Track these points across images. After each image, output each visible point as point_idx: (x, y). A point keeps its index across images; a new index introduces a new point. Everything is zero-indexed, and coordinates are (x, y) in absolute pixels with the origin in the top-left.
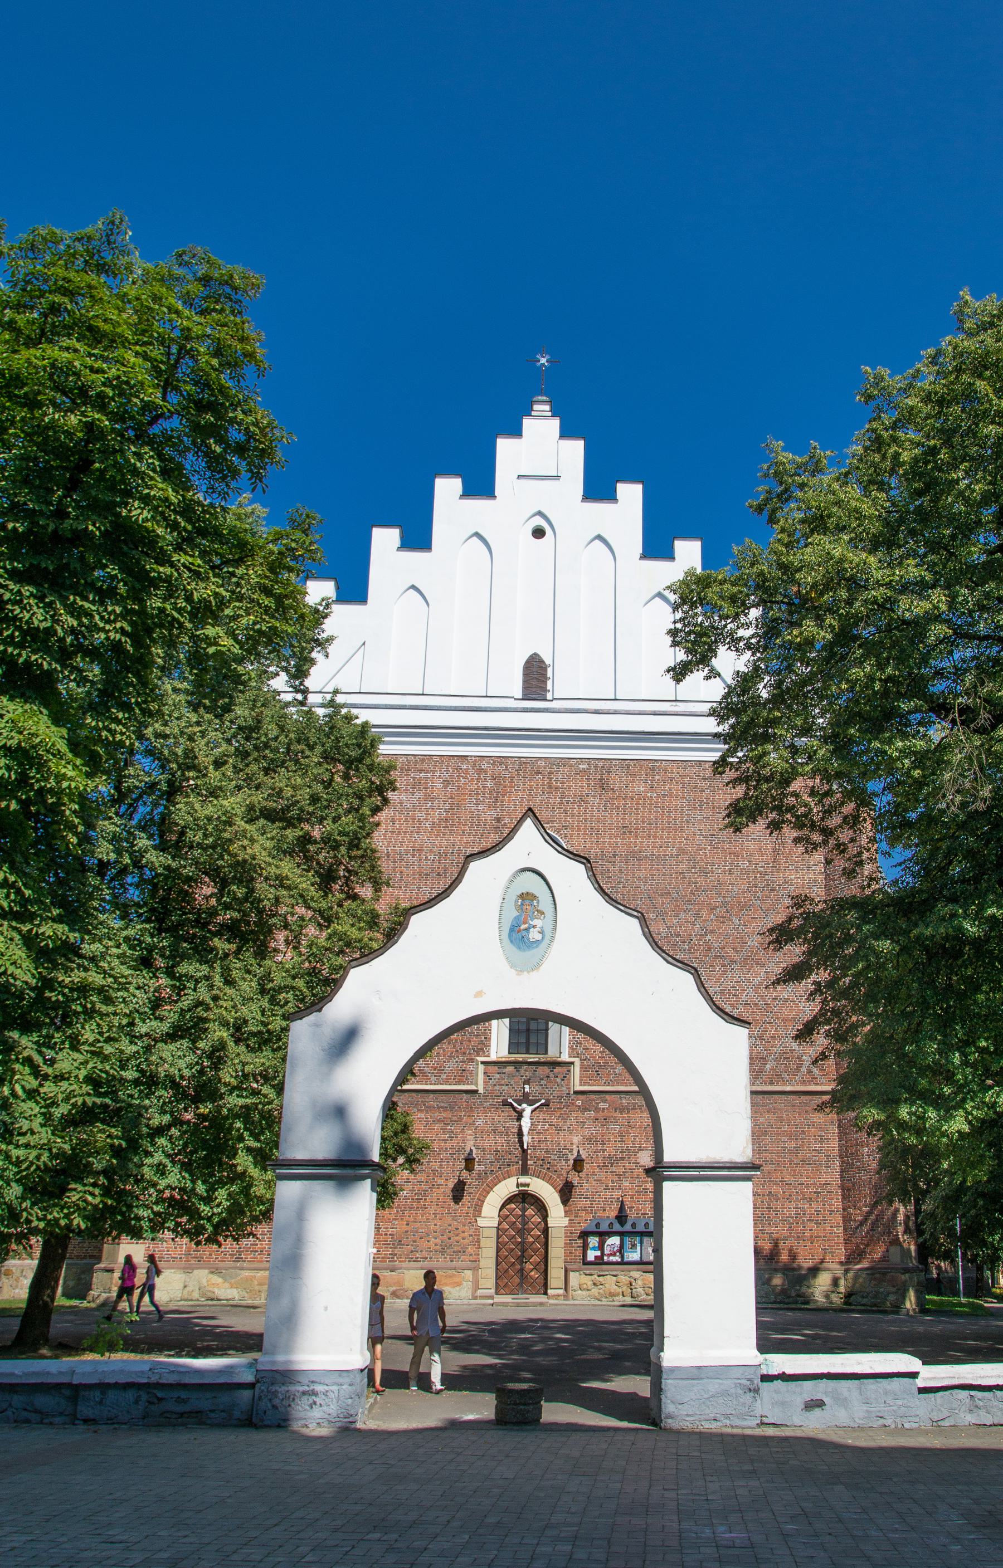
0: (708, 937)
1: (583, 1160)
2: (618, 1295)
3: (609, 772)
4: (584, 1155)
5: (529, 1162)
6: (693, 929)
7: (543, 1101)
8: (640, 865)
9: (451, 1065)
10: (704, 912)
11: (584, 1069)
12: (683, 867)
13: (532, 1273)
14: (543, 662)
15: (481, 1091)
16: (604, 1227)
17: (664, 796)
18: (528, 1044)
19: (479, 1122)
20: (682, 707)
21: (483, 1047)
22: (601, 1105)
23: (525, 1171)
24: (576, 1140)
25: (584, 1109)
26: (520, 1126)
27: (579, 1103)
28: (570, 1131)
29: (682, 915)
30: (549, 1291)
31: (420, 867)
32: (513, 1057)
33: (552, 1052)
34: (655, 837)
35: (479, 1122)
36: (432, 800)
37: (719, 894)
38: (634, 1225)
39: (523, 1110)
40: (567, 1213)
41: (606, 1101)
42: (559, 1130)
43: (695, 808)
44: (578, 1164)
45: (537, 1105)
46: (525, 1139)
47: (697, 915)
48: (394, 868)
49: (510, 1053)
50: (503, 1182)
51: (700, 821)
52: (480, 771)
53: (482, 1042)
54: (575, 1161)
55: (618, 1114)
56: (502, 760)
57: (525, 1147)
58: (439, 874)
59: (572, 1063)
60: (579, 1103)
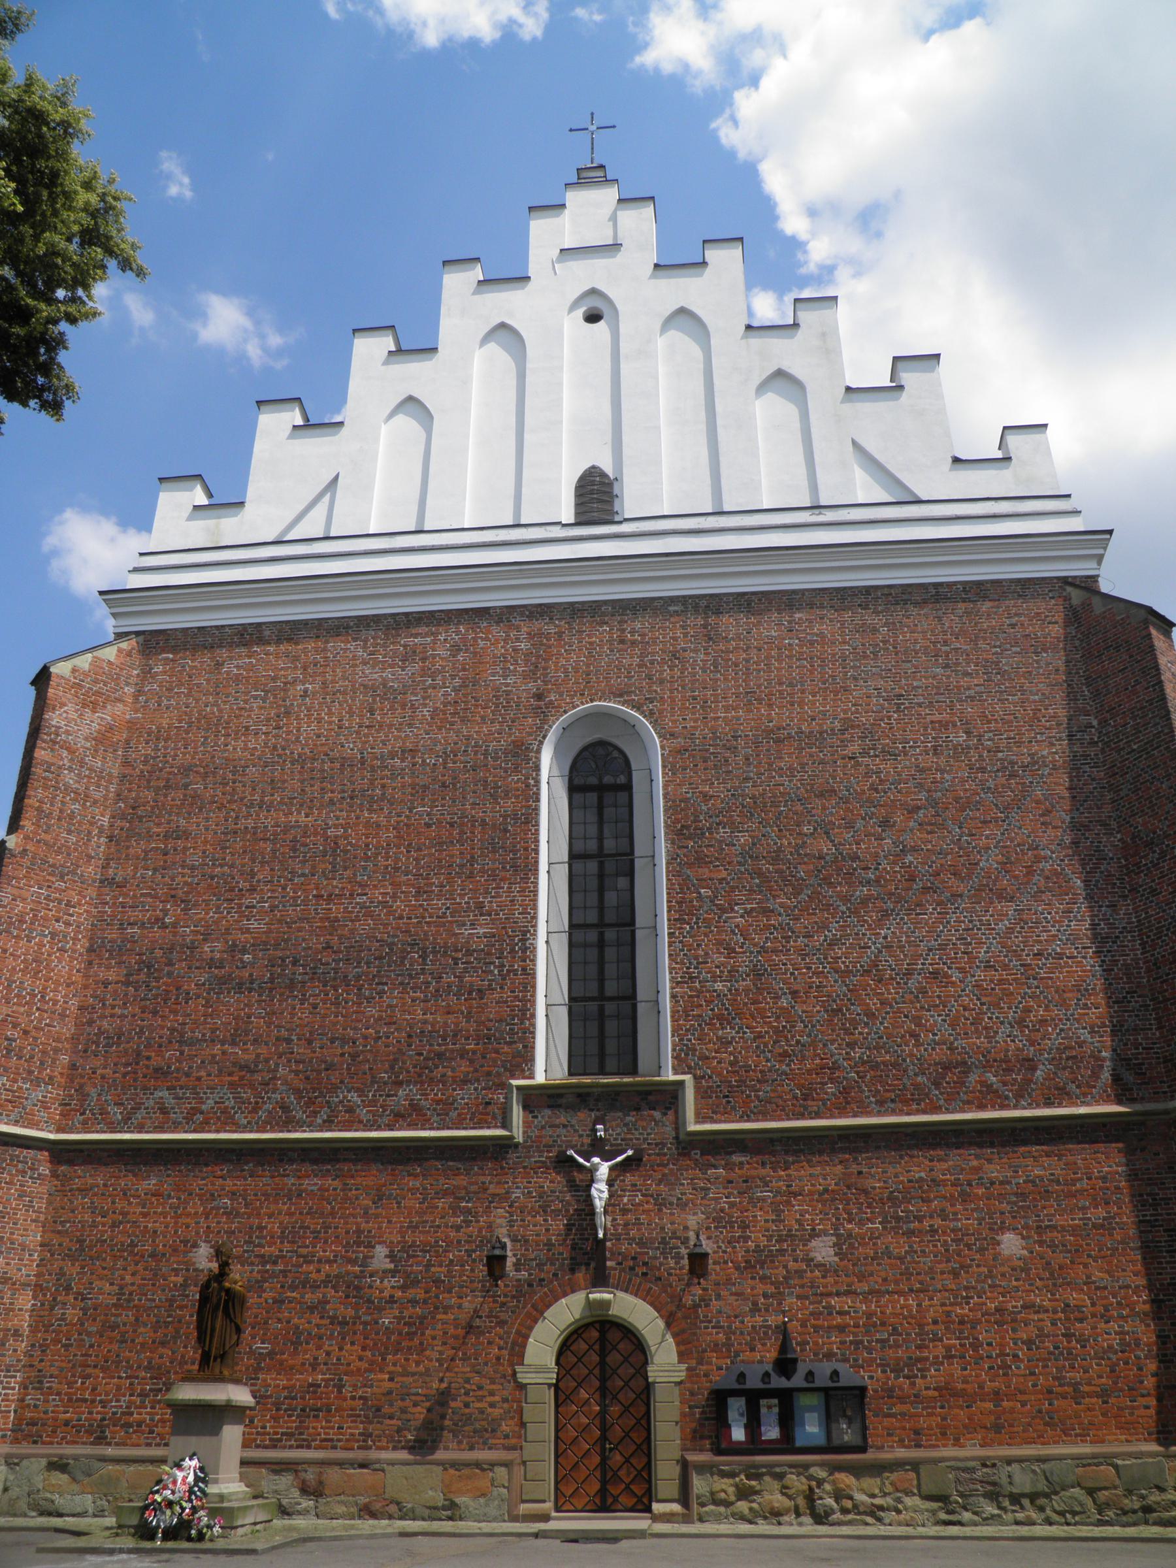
0: (909, 858)
1: (706, 1255)
2: (787, 1511)
4: (707, 1246)
5: (609, 1263)
7: (630, 1153)
8: (779, 751)
9: (464, 1096)
10: (898, 818)
12: (854, 748)
14: (606, 476)
16: (754, 1383)
17: (812, 643)
18: (602, 1055)
19: (517, 1193)
20: (829, 516)
21: (523, 1061)
23: (600, 1280)
24: (693, 1221)
28: (682, 1205)
29: (859, 824)
30: (657, 1507)
32: (574, 1080)
34: (801, 704)
35: (517, 1193)
37: (920, 786)
38: (810, 1375)
42: (661, 1203)
43: (865, 657)
45: (619, 1159)
46: (601, 1220)
47: (885, 823)
48: (372, 782)
49: (571, 1074)
53: (517, 1055)
54: (692, 1257)
55: (766, 1171)
57: (601, 1235)
58: (444, 785)
59: (682, 1083)
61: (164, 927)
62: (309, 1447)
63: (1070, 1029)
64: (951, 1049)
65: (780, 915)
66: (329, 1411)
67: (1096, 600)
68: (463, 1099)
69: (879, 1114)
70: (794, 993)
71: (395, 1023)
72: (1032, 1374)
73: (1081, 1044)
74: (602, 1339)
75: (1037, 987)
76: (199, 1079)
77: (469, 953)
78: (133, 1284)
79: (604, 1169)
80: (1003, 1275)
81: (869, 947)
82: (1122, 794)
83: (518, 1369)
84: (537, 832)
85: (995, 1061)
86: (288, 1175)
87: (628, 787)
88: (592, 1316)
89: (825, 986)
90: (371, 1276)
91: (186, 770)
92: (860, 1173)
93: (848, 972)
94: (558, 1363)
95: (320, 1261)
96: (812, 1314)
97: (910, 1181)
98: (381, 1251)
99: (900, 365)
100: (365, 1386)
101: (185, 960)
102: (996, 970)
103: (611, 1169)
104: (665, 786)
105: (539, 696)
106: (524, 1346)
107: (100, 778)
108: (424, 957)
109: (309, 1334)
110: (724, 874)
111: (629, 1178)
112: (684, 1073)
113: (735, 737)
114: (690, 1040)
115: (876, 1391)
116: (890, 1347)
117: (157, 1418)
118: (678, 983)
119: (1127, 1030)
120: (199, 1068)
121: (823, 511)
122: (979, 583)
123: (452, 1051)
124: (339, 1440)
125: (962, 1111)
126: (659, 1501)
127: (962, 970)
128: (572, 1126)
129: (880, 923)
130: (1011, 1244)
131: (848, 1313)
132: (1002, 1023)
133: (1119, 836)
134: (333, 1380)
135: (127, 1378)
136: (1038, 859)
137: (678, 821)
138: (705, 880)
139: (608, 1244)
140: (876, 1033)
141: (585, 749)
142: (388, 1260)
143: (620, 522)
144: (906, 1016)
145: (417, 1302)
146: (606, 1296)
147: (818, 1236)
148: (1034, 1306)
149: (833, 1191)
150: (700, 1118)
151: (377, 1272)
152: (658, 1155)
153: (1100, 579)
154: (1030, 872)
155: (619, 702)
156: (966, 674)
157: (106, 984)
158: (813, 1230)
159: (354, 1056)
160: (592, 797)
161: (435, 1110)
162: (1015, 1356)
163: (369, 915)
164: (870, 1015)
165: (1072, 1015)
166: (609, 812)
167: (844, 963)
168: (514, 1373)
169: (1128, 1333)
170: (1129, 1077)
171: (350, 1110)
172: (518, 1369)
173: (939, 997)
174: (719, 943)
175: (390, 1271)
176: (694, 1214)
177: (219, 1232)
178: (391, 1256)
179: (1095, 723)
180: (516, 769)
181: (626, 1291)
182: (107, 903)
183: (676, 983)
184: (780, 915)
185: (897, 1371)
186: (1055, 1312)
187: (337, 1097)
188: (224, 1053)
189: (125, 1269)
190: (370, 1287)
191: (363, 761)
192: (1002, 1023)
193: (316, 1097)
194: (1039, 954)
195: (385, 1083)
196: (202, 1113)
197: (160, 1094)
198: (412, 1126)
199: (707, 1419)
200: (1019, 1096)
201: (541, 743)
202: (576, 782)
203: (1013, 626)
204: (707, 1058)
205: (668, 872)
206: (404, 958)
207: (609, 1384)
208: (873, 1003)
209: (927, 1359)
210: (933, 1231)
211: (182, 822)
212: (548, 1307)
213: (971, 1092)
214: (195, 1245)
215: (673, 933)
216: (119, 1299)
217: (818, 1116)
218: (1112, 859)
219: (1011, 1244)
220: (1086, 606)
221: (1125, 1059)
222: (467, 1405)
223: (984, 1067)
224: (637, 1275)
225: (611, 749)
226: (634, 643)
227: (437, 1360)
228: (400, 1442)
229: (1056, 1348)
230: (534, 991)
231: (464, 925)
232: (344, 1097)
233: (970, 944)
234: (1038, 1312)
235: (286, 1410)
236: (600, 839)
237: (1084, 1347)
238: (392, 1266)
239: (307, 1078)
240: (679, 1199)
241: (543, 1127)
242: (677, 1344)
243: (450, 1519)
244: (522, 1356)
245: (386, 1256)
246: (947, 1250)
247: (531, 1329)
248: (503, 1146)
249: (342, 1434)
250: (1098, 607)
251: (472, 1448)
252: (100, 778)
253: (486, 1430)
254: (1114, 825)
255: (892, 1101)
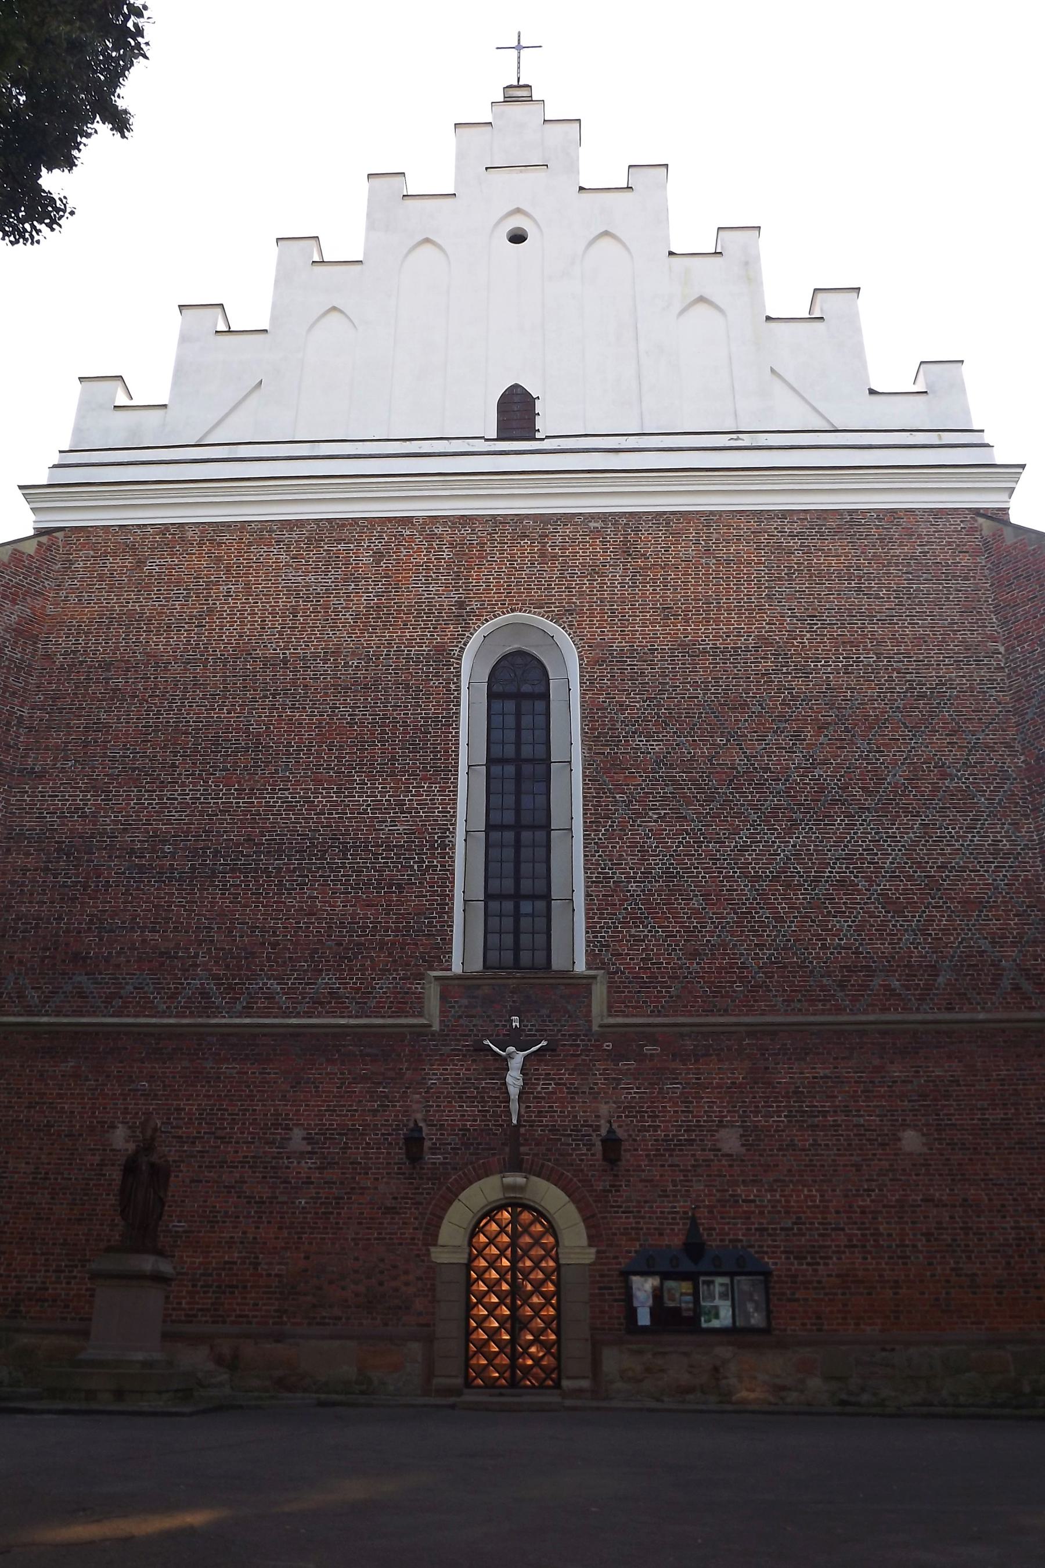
1: (619, 1141)
3: (637, 530)
4: (621, 1133)
6: (791, 759)
7: (544, 1043)
10: (809, 732)
11: (613, 988)
13: (533, 1349)
15: (436, 1027)
17: (728, 561)
20: (746, 440)
22: (648, 1049)
23: (516, 1165)
24: (604, 1109)
25: (617, 1056)
26: (505, 1084)
27: (608, 1046)
30: (566, 1383)
31: (335, 677)
33: (558, 963)
34: (717, 622)
36: (356, 581)
39: (510, 1056)
40: (592, 1240)
41: (655, 1043)
43: (780, 579)
44: (612, 1146)
46: (514, 1106)
47: (797, 736)
50: (475, 1186)
51: (790, 598)
52: (432, 536)
56: (465, 520)
57: (515, 1122)
58: (366, 687)
59: (594, 977)
60: (608, 1046)
61: (84, 816)
62: (224, 1322)
63: (971, 939)
64: (857, 953)
65: (693, 821)
66: (245, 1287)
67: (1007, 532)
68: (381, 988)
69: (786, 1013)
70: (706, 895)
71: (315, 914)
72: (930, 1264)
73: (982, 953)
74: (514, 1221)
75: (940, 898)
76: (118, 966)
77: (389, 849)
78: (49, 1164)
79: (518, 1059)
80: (904, 1170)
81: (779, 855)
82: (1027, 718)
83: (432, 1249)
84: (457, 735)
85: (898, 966)
86: (207, 1059)
87: (546, 696)
88: (507, 1198)
89: (736, 890)
90: (288, 1158)
91: (107, 666)
92: (767, 1068)
93: (757, 878)
94: (470, 1244)
95: (237, 1143)
96: (719, 1201)
97: (814, 1078)
98: (298, 1134)
99: (820, 296)
100: (280, 1264)
101: (105, 849)
102: (902, 881)
103: (526, 1058)
104: (583, 695)
105: (461, 605)
106: (438, 1227)
107: (20, 669)
108: (344, 851)
109: (226, 1212)
110: (639, 781)
111: (543, 1068)
112: (597, 969)
113: (652, 651)
114: (604, 937)
115: (779, 1276)
116: (794, 1235)
117: (72, 1293)
118: (593, 882)
119: (1027, 942)
120: (119, 954)
121: (741, 436)
122: (893, 511)
123: (371, 942)
124: (255, 1317)
125: (865, 1012)
126: (568, 1378)
127: (868, 879)
128: (488, 1017)
129: (789, 832)
130: (911, 1140)
131: (754, 1201)
132: (906, 930)
133: (1022, 758)
134: (249, 1258)
135: (43, 1254)
136: (944, 776)
137: (593, 729)
138: (621, 785)
139: (522, 1130)
140: (784, 936)
141: (504, 658)
142: (305, 1142)
143: (543, 439)
144: (813, 921)
145: (334, 1183)
146: (519, 1180)
147: (725, 1126)
148: (932, 1200)
149: (741, 1083)
150: (611, 1011)
151: (295, 1152)
152: (571, 1045)
153: (1010, 512)
154: (936, 789)
155: (539, 614)
156: (877, 597)
157: (25, 870)
158: (721, 1121)
159: (274, 945)
160: (510, 706)
161: (353, 998)
162: (914, 1246)
163: (290, 808)
164: (779, 919)
165: (974, 925)
166: (526, 721)
167: (753, 868)
168: (428, 1253)
169: (1023, 1228)
170: (1027, 986)
171: (270, 998)
172: (432, 1249)
173: (844, 903)
174: (633, 845)
175: (308, 1153)
176: (606, 1103)
177: (137, 1113)
178: (308, 1139)
179: (1002, 649)
180: (437, 675)
181: (539, 1176)
182: (27, 792)
183: (589, 883)
184: (693, 821)
185: (800, 1258)
186: (955, 1206)
187: (257, 984)
188: (144, 941)
189: (41, 1149)
190: (288, 1168)
191: (285, 661)
192: (906, 930)
193: (236, 984)
194: (942, 867)
195: (307, 971)
196: (121, 998)
197: (79, 979)
198: (331, 1014)
199: (616, 1300)
200: (921, 999)
201: (462, 649)
202: (495, 689)
203: (925, 553)
204: (621, 955)
205: (584, 776)
206: (326, 851)
207: (520, 1265)
208: (783, 908)
209: (830, 1246)
210: (836, 1126)
211: (103, 716)
212: (464, 1189)
213: (875, 995)
214: (113, 1127)
215: (589, 835)
216: (34, 1178)
217: (726, 1012)
218: (1015, 779)
219: (911, 1140)
220: (997, 536)
221: (1024, 970)
222: (381, 1284)
223: (889, 971)
224: (549, 1160)
225: (529, 659)
226: (555, 557)
227: (353, 1239)
228: (315, 1318)
229: (955, 1240)
230: (453, 887)
231: (384, 822)
232: (264, 984)
233: (876, 854)
234: (937, 1206)
235: (202, 1287)
236: (518, 744)
237: (980, 1240)
238: (309, 1148)
239: (227, 966)
240: (591, 1088)
241: (460, 1017)
242: (587, 1227)
243: (362, 1393)
244: (436, 1236)
245: (304, 1139)
246: (850, 1145)
247: (445, 1210)
248: (421, 1032)
249: (257, 1310)
250: (1010, 539)
251: (386, 1325)
252: (20, 669)
253: (400, 1308)
254: (1018, 747)
255: (799, 1001)
